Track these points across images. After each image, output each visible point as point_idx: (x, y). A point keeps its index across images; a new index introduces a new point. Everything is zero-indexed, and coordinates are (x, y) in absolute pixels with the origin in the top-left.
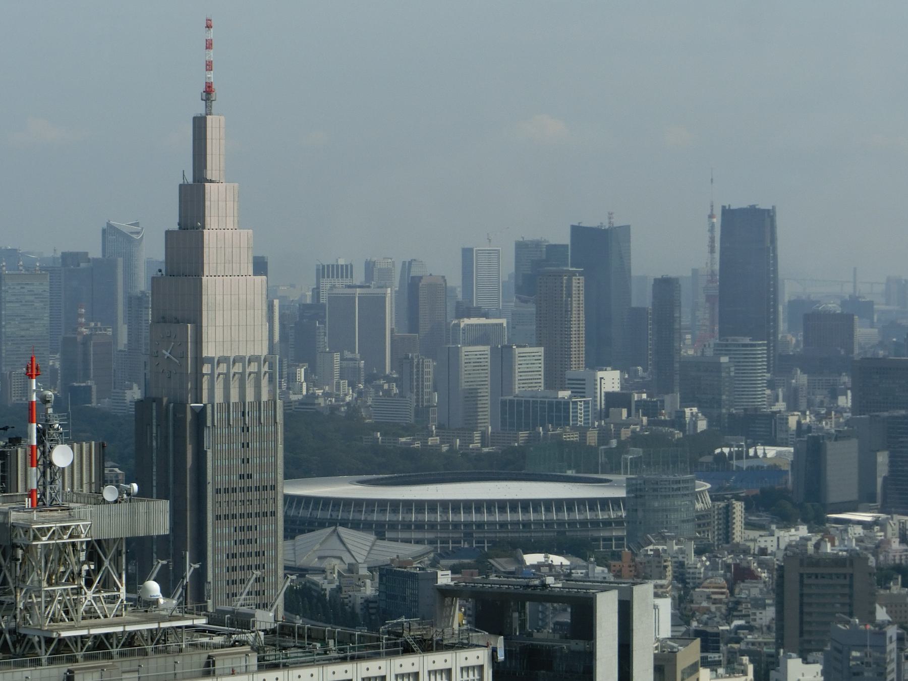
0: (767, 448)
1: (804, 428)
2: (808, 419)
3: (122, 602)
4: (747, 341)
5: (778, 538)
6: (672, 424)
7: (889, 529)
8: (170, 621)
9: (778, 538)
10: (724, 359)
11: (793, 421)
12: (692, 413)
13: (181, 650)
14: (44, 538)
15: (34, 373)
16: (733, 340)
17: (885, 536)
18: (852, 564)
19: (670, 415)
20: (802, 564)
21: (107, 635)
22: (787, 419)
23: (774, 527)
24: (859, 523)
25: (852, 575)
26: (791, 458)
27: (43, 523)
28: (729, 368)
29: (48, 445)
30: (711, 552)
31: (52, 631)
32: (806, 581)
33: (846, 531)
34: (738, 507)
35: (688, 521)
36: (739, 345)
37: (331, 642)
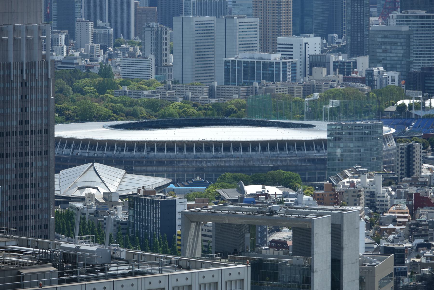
6: (362, 80)
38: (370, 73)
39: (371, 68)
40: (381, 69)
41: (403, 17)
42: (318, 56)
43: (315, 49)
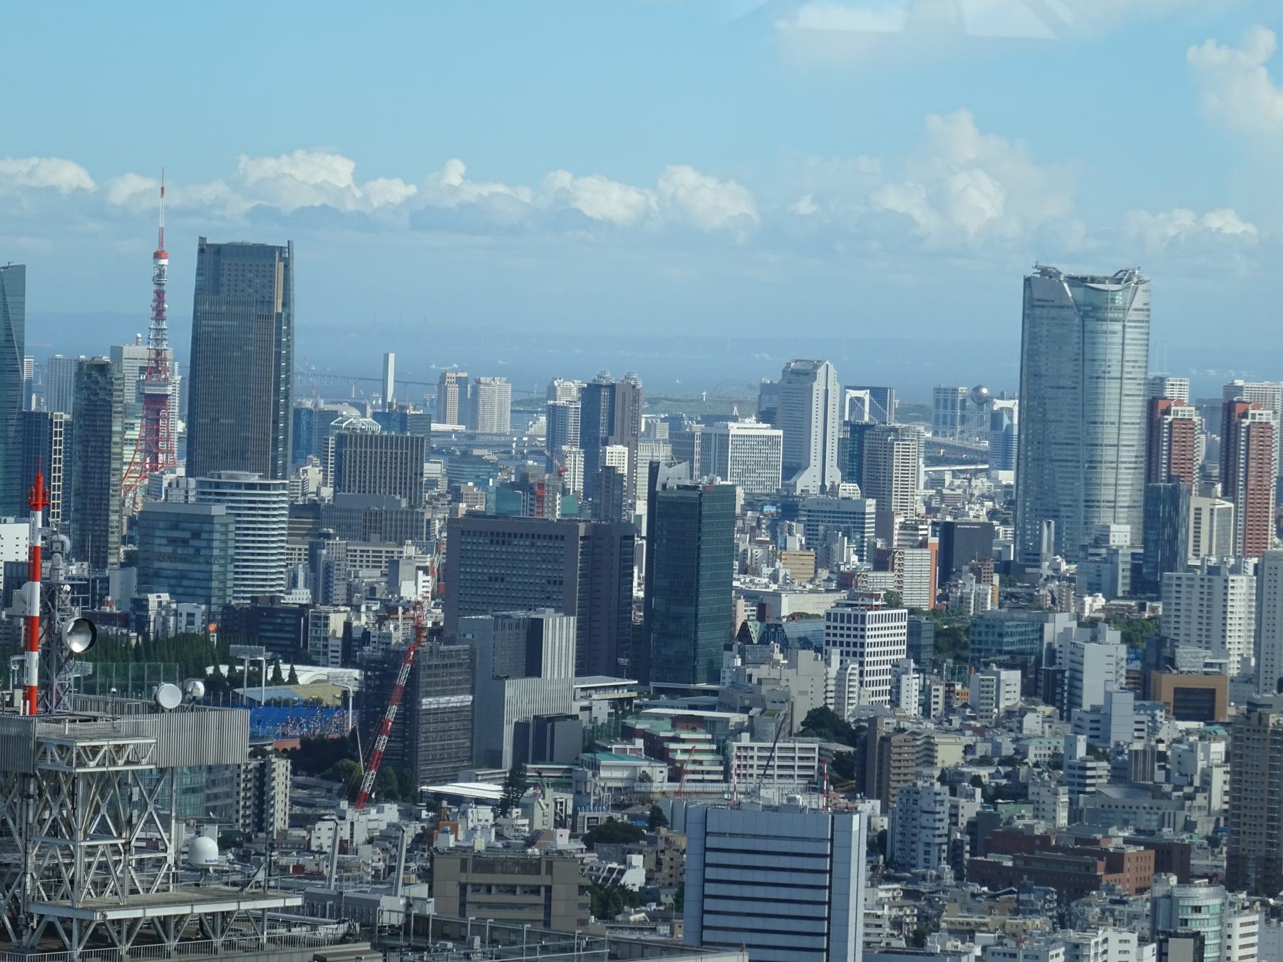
0: (296, 667)
1: (357, 635)
2: (364, 619)
3: (169, 868)
4: (255, 479)
5: (352, 824)
6: (124, 620)
7: (538, 812)
8: (254, 899)
9: (352, 824)
10: (218, 510)
11: (337, 622)
12: (160, 603)
13: (260, 947)
14: (92, 764)
15: (40, 502)
16: (232, 477)
17: (531, 825)
18: (550, 871)
19: (119, 603)
20: (464, 868)
21: (164, 921)
22: (327, 618)
23: (344, 804)
24: (479, 801)
25: (549, 889)
26: (353, 688)
27: (91, 739)
28: (226, 525)
29: (58, 616)
30: (239, 845)
31: (94, 910)
32: (471, 897)
33: (464, 814)
34: (281, 769)
35: (194, 791)
36: (239, 486)
37: (477, 940)
38: (141, 605)
39: (142, 596)
40: (165, 597)
41: (210, 484)
42: (22, 563)
43: (17, 549)
